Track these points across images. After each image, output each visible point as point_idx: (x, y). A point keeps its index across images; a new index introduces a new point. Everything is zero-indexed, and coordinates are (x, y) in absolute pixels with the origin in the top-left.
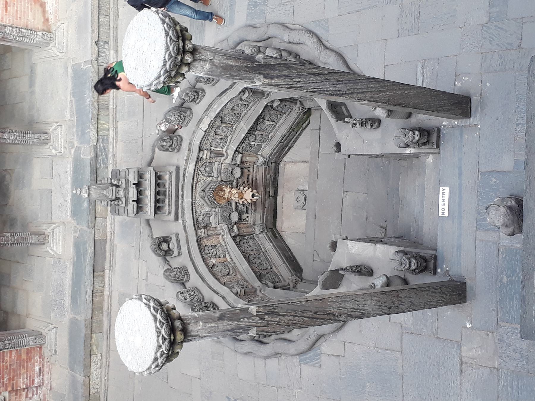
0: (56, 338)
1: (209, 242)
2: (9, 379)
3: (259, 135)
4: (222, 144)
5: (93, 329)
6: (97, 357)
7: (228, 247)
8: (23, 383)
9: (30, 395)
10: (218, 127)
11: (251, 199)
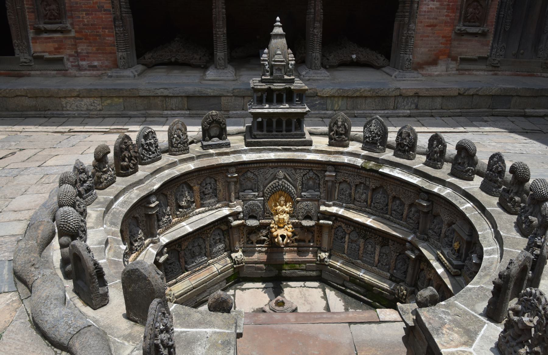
0: (123, 77)
1: (220, 186)
3: (359, 245)
6: (99, 105)
8: (82, 50)
9: (71, 59)
10: (367, 187)
11: (277, 235)
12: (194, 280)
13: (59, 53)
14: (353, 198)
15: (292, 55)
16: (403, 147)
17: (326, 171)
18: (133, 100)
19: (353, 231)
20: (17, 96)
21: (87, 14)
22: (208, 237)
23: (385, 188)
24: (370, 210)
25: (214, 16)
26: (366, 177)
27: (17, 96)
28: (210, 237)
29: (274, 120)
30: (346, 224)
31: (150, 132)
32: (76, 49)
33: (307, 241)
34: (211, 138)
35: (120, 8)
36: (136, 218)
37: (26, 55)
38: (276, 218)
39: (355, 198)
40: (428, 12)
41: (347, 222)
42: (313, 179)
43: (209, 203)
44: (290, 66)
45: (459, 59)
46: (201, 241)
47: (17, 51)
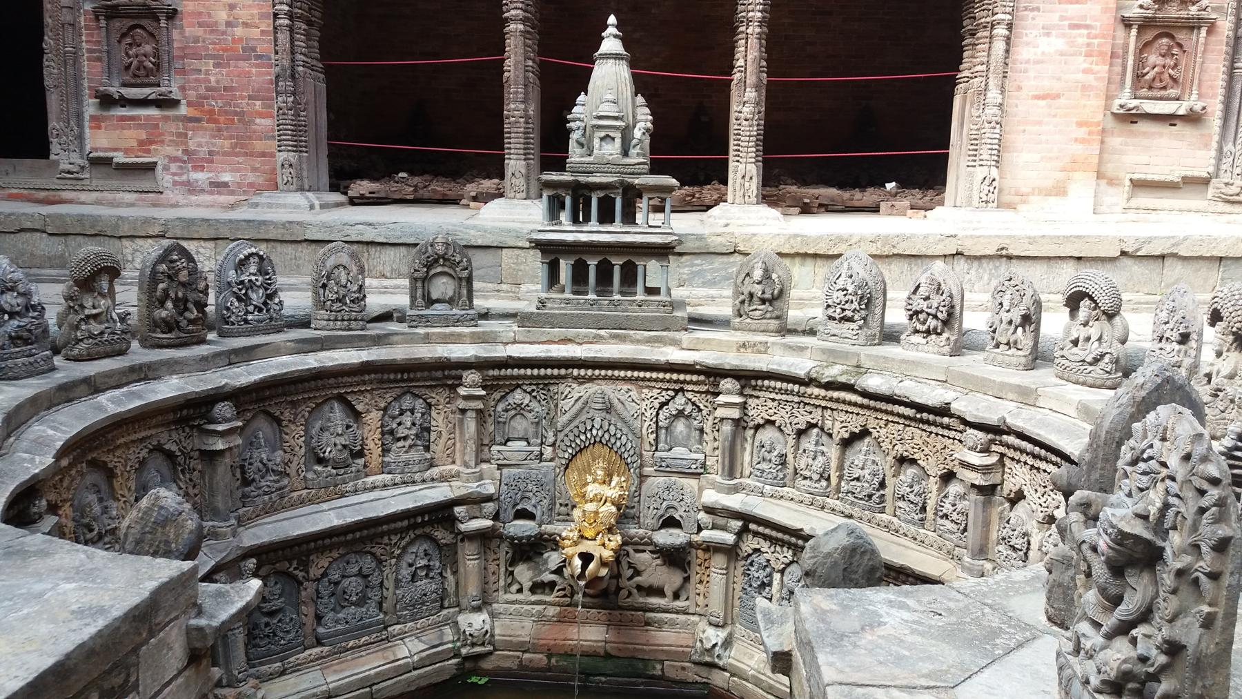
0: (285, 206)
2: (211, 112)
4: (764, 466)
5: (278, 245)
7: (417, 488)
8: (200, 145)
9: (174, 167)
12: (336, 672)
13: (148, 151)
14: (790, 471)
15: (647, 111)
16: (924, 323)
17: (717, 394)
18: (290, 249)
19: (792, 562)
20: (22, 230)
21: (216, 65)
22: (392, 555)
23: (875, 434)
24: (838, 502)
25: (506, 74)
26: (825, 408)
27: (22, 230)
28: (399, 557)
29: (592, 263)
30: (773, 541)
31: (251, 255)
32: (186, 144)
33: (669, 591)
34: (430, 302)
35: (293, 53)
36: (170, 456)
37: (73, 155)
38: (577, 513)
39: (796, 469)
40: (1037, 62)
41: (774, 534)
42: (689, 417)
43: (407, 463)
44: (636, 130)
45: (1128, 183)
46: (368, 563)
47: (55, 147)
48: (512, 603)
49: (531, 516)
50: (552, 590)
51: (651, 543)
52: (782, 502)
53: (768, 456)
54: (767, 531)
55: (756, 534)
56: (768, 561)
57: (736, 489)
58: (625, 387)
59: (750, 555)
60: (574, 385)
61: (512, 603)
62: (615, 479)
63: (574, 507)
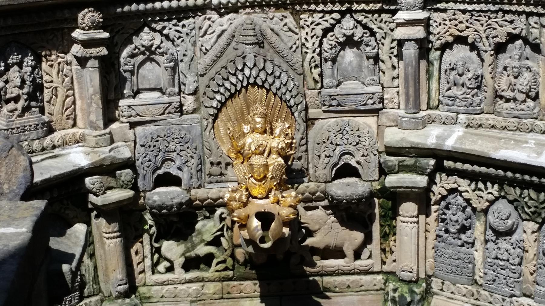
4: (455, 91)
17: (393, 13)
19: (497, 199)
26: (529, 15)
33: (349, 251)
48: (163, 284)
49: (175, 181)
50: (209, 265)
51: (326, 195)
52: (481, 131)
53: (461, 80)
54: (467, 167)
55: (450, 172)
56: (468, 201)
57: (424, 123)
58: (279, 14)
59: (444, 198)
60: (214, 16)
61: (163, 284)
62: (278, 128)
63: (228, 164)
